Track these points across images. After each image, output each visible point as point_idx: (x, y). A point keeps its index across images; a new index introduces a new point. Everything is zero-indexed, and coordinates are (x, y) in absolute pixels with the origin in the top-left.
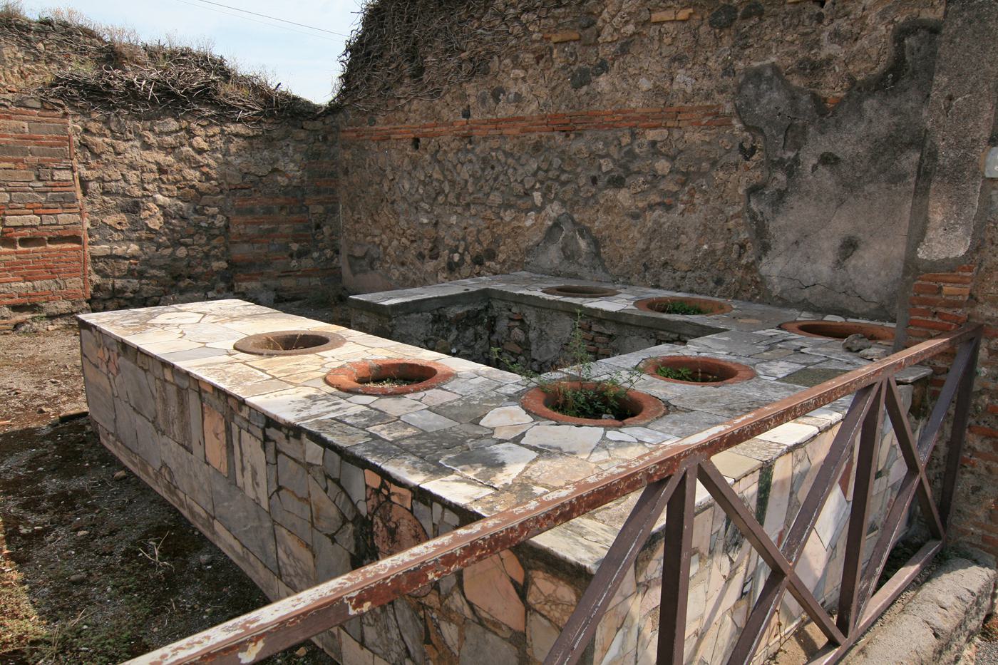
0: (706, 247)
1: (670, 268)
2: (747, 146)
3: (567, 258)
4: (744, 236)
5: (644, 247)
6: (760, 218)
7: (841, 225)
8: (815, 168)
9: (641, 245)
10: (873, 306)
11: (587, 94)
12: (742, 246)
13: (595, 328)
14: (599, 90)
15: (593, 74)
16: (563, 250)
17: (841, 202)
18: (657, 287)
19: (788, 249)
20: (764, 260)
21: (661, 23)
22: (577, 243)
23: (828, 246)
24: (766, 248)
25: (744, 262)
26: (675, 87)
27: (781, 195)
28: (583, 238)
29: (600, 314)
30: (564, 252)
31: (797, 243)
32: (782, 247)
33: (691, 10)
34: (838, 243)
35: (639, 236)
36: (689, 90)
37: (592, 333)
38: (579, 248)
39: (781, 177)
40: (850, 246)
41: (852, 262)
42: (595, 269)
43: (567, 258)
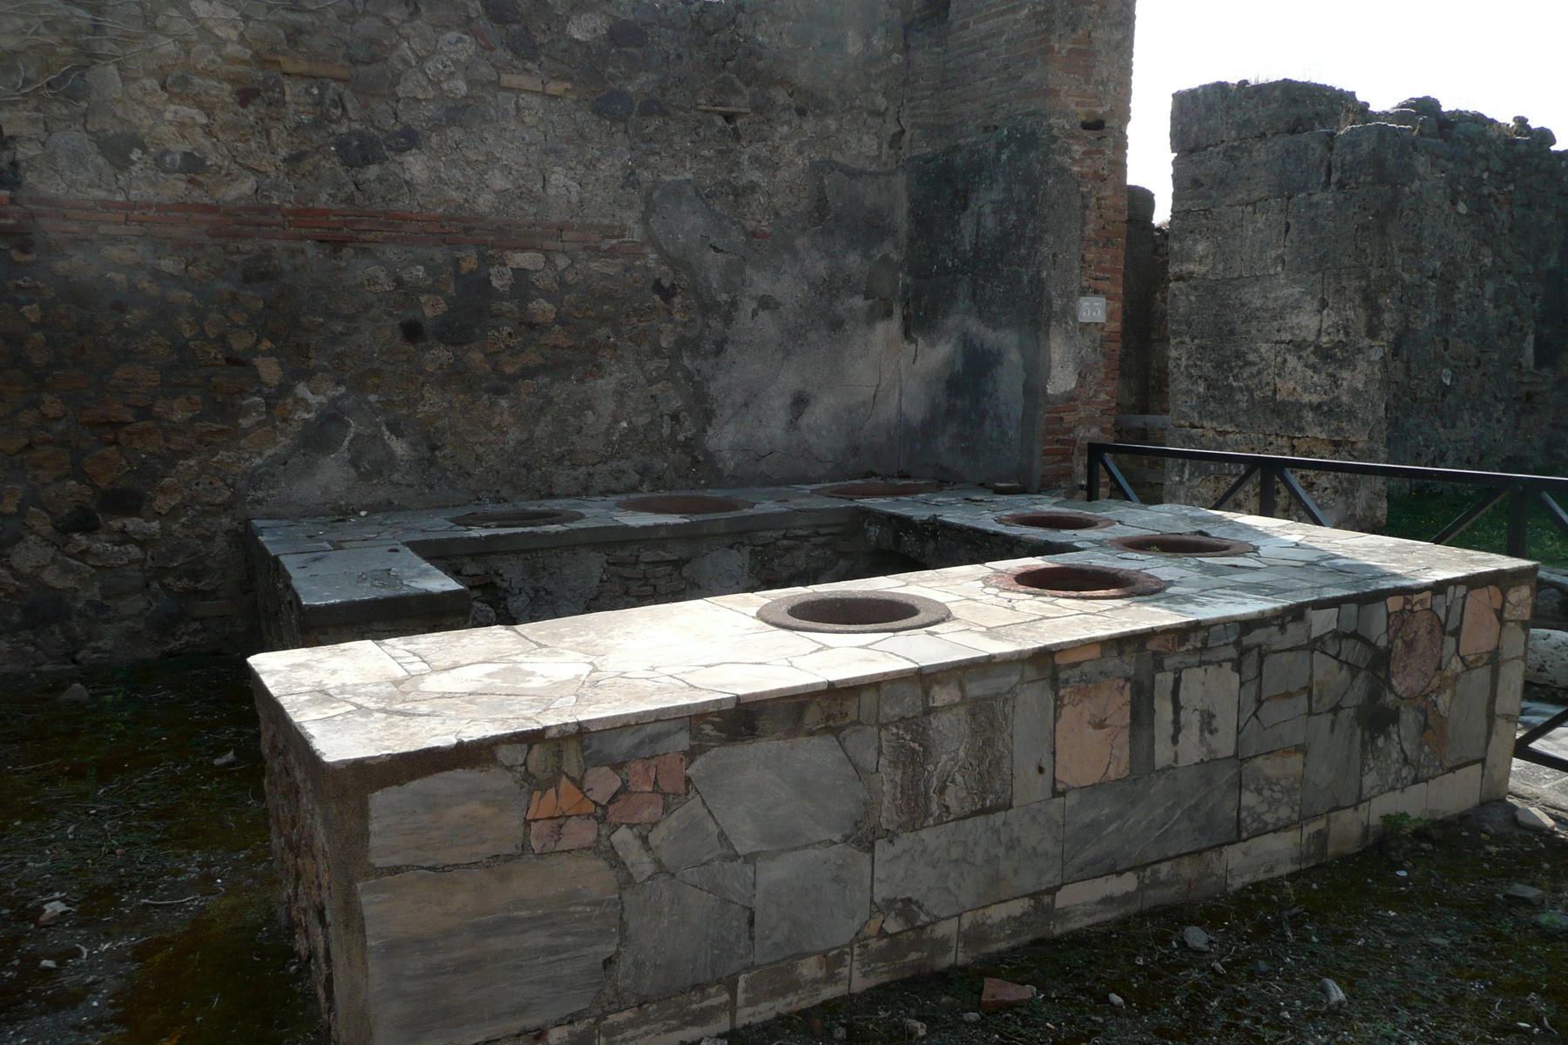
0: (625, 424)
1: (567, 463)
2: (666, 283)
3: (364, 477)
4: (677, 403)
5: (525, 436)
6: (697, 378)
7: (790, 379)
8: (755, 314)
9: (514, 435)
10: (829, 466)
11: (380, 180)
12: (675, 417)
13: (648, 556)
14: (407, 177)
15: (390, 148)
16: (354, 463)
17: (788, 354)
18: (551, 496)
19: (736, 414)
20: (710, 432)
21: (518, 91)
22: (385, 445)
23: (777, 406)
24: (709, 415)
25: (681, 437)
26: (552, 192)
27: (720, 348)
28: (400, 435)
29: (663, 533)
30: (357, 467)
31: (746, 405)
32: (729, 412)
33: (568, 85)
34: (789, 401)
35: (511, 420)
36: (574, 198)
37: (642, 567)
38: (391, 455)
39: (716, 324)
40: (800, 402)
41: (805, 420)
42: (431, 487)
43: (364, 477)
